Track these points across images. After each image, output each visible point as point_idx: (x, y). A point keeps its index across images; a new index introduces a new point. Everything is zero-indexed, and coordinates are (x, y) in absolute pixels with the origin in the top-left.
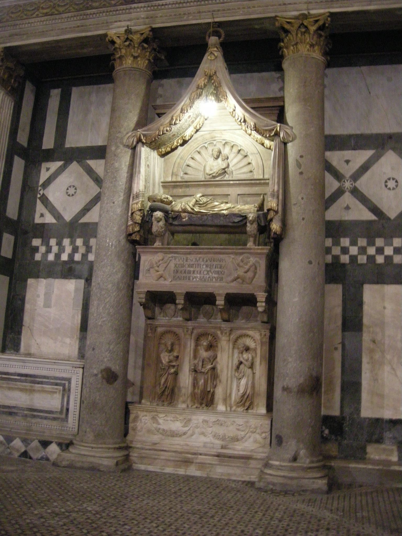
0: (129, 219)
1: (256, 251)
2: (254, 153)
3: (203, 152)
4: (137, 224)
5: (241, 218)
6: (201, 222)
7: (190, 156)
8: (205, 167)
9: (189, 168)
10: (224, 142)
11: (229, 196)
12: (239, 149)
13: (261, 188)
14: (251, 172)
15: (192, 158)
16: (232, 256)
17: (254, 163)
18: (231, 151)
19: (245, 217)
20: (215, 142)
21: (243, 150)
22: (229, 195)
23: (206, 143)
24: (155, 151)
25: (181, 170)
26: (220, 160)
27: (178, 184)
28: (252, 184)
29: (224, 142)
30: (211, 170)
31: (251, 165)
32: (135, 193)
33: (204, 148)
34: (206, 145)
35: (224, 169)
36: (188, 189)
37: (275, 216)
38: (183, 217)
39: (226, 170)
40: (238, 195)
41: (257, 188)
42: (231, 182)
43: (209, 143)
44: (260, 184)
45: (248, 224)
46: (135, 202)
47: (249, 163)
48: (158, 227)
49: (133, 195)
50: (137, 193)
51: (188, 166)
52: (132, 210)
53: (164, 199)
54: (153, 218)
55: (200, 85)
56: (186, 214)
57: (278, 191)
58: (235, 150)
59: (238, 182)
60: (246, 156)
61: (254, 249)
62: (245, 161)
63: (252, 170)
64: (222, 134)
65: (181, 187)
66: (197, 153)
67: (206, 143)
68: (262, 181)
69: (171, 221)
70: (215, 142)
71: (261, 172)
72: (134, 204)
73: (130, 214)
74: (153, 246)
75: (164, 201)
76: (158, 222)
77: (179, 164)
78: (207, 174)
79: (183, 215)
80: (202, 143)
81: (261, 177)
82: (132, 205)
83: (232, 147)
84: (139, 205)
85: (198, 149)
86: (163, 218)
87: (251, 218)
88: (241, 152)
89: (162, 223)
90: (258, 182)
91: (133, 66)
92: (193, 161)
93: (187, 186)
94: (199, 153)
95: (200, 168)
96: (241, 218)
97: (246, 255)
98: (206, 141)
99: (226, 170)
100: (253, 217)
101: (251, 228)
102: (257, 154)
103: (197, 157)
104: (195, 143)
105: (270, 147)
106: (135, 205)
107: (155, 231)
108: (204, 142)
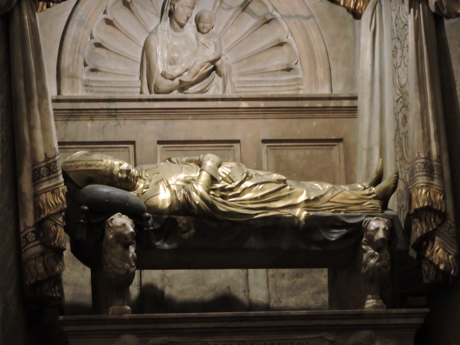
0: (31, 237)
1: (392, 321)
2: (297, 16)
5: (344, 231)
8: (146, 49)
9: (98, 50)
11: (236, 145)
13: (326, 120)
15: (109, 22)
16: (330, 338)
17: (296, 43)
22: (238, 141)
27: (82, 105)
28: (300, 110)
30: (172, 62)
35: (213, 62)
36: (112, 123)
37: (439, 226)
39: (218, 63)
40: (264, 141)
41: (315, 123)
42: (244, 104)
44: (324, 110)
49: (34, 162)
50: (47, 158)
51: (98, 45)
52: (38, 210)
57: (440, 157)
59: (262, 104)
60: (268, 21)
61: (388, 316)
62: (268, 37)
63: (293, 65)
65: (92, 114)
68: (332, 104)
71: (321, 73)
73: (29, 220)
74: (103, 316)
77: (75, 41)
78: (164, 75)
84: (62, 195)
87: (381, 235)
88: (251, 6)
92: (110, 28)
93: (112, 114)
95: (129, 52)
96: (344, 231)
97: (365, 333)
100: (384, 229)
102: (308, 18)
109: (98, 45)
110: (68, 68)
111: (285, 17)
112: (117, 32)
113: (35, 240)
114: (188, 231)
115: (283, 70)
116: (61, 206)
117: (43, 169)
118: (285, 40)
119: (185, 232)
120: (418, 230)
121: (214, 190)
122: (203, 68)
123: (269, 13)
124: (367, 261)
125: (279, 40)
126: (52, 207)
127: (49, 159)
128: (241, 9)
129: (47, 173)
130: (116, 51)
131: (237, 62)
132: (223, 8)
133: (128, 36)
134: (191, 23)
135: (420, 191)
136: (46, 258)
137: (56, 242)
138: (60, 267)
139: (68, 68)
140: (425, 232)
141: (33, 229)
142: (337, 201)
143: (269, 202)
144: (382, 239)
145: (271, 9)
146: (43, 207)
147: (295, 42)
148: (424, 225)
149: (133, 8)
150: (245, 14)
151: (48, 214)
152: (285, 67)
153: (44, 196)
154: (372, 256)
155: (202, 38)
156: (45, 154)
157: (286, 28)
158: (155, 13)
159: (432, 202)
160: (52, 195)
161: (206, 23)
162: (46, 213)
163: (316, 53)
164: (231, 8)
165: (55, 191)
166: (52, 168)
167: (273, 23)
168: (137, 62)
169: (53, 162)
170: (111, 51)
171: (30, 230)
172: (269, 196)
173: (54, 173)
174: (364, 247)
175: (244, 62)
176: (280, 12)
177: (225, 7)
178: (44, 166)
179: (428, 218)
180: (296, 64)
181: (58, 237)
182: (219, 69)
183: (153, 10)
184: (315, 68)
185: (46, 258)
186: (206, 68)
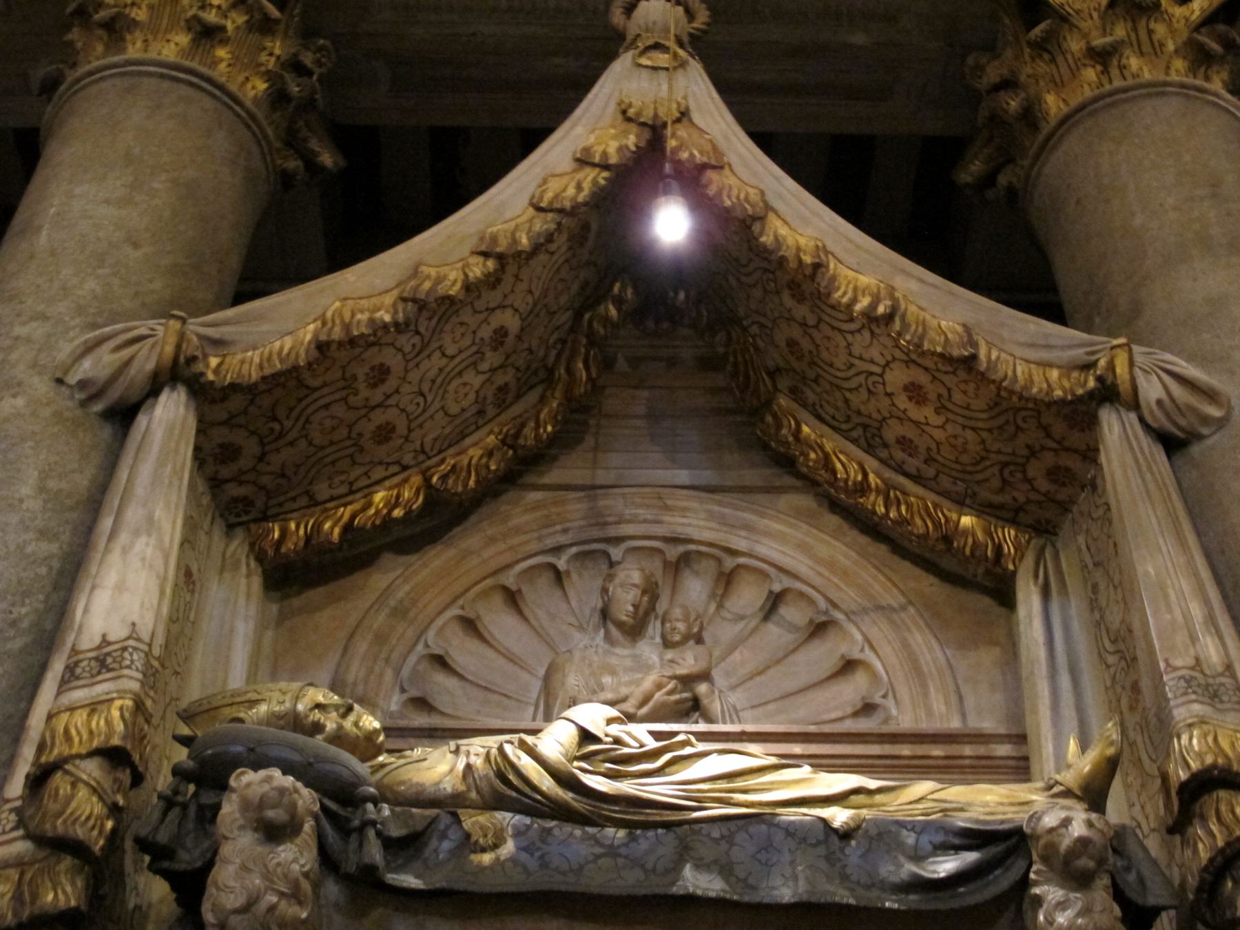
3: (540, 598)
4: (67, 862)
5: (971, 857)
6: (629, 881)
7: (455, 611)
10: (681, 549)
12: (777, 588)
14: (868, 708)
18: (720, 606)
19: (1004, 845)
20: (616, 553)
21: (802, 595)
23: (557, 550)
24: (240, 534)
25: (389, 674)
26: (648, 650)
29: (673, 552)
31: (860, 679)
32: (89, 640)
33: (545, 580)
34: (561, 564)
35: (687, 681)
38: (477, 836)
43: (578, 556)
45: (1050, 892)
46: (78, 695)
47: (848, 666)
48: (267, 876)
49: (74, 651)
50: (105, 642)
52: (41, 748)
53: (317, 715)
54: (229, 808)
55: (599, 149)
56: (506, 818)
58: (748, 597)
60: (819, 629)
63: (877, 699)
64: (667, 508)
66: (498, 600)
67: (557, 550)
68: (968, 750)
69: (375, 853)
70: (616, 553)
72: (72, 709)
75: (317, 728)
76: (274, 833)
79: (473, 821)
80: (534, 546)
81: (955, 724)
82: (50, 717)
83: (726, 580)
84: (116, 714)
85: (509, 579)
86: (309, 826)
89: (296, 857)
90: (937, 751)
91: (187, 63)
92: (473, 644)
94: (513, 599)
96: (971, 857)
98: (563, 539)
99: (702, 688)
101: (1086, 911)
102: (903, 608)
103: (501, 623)
104: (492, 540)
105: (998, 549)
106: (80, 717)
107: (232, 901)
108: (550, 542)
109: (441, 662)
110: (355, 684)
111: (854, 613)
112: (490, 653)
113: (13, 829)
114: (495, 846)
115: (856, 714)
116: (103, 737)
117: (85, 663)
118: (856, 655)
119: (483, 850)
120: (1200, 846)
121: (584, 758)
122: (664, 690)
123: (819, 612)
124: (1050, 922)
125: (843, 656)
126: (76, 740)
127: (109, 644)
128: (761, 615)
129: (94, 672)
130: (483, 684)
131: (753, 707)
132: (724, 619)
133: (511, 658)
134: (653, 638)
135: (1185, 738)
136: (28, 876)
137: (60, 821)
138: (61, 897)
139: (355, 684)
140: (1220, 843)
141: (18, 803)
142: (949, 798)
143: (745, 791)
144: (1083, 842)
145: (822, 604)
146: (53, 738)
147: (879, 656)
148: (1214, 828)
149: (527, 612)
150: (772, 629)
151: (60, 754)
152: (859, 706)
153: (65, 717)
154: (1062, 906)
155: (670, 655)
156: (104, 636)
157: (859, 637)
158: (576, 624)
159: (1226, 756)
160: (89, 715)
161: (678, 620)
162: (56, 752)
163: (925, 669)
164: (742, 618)
165: (99, 707)
166: (109, 660)
167: (832, 634)
168: (527, 703)
169: (116, 651)
170: (472, 682)
171: (8, 806)
172: (746, 777)
173: (109, 670)
174: (1037, 890)
175: (771, 707)
176: (843, 606)
177: (729, 616)
178: (90, 659)
179: (1223, 808)
180: (884, 697)
181: (69, 811)
182: (705, 702)
183: (572, 620)
184: (926, 695)
185: (28, 876)
186: (671, 693)
